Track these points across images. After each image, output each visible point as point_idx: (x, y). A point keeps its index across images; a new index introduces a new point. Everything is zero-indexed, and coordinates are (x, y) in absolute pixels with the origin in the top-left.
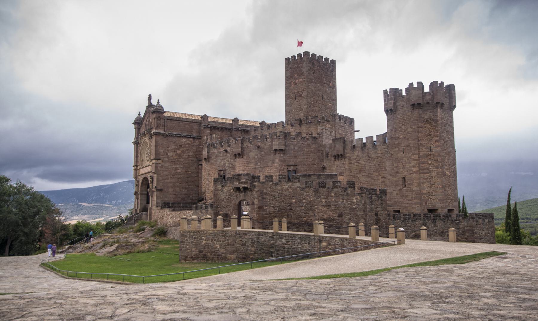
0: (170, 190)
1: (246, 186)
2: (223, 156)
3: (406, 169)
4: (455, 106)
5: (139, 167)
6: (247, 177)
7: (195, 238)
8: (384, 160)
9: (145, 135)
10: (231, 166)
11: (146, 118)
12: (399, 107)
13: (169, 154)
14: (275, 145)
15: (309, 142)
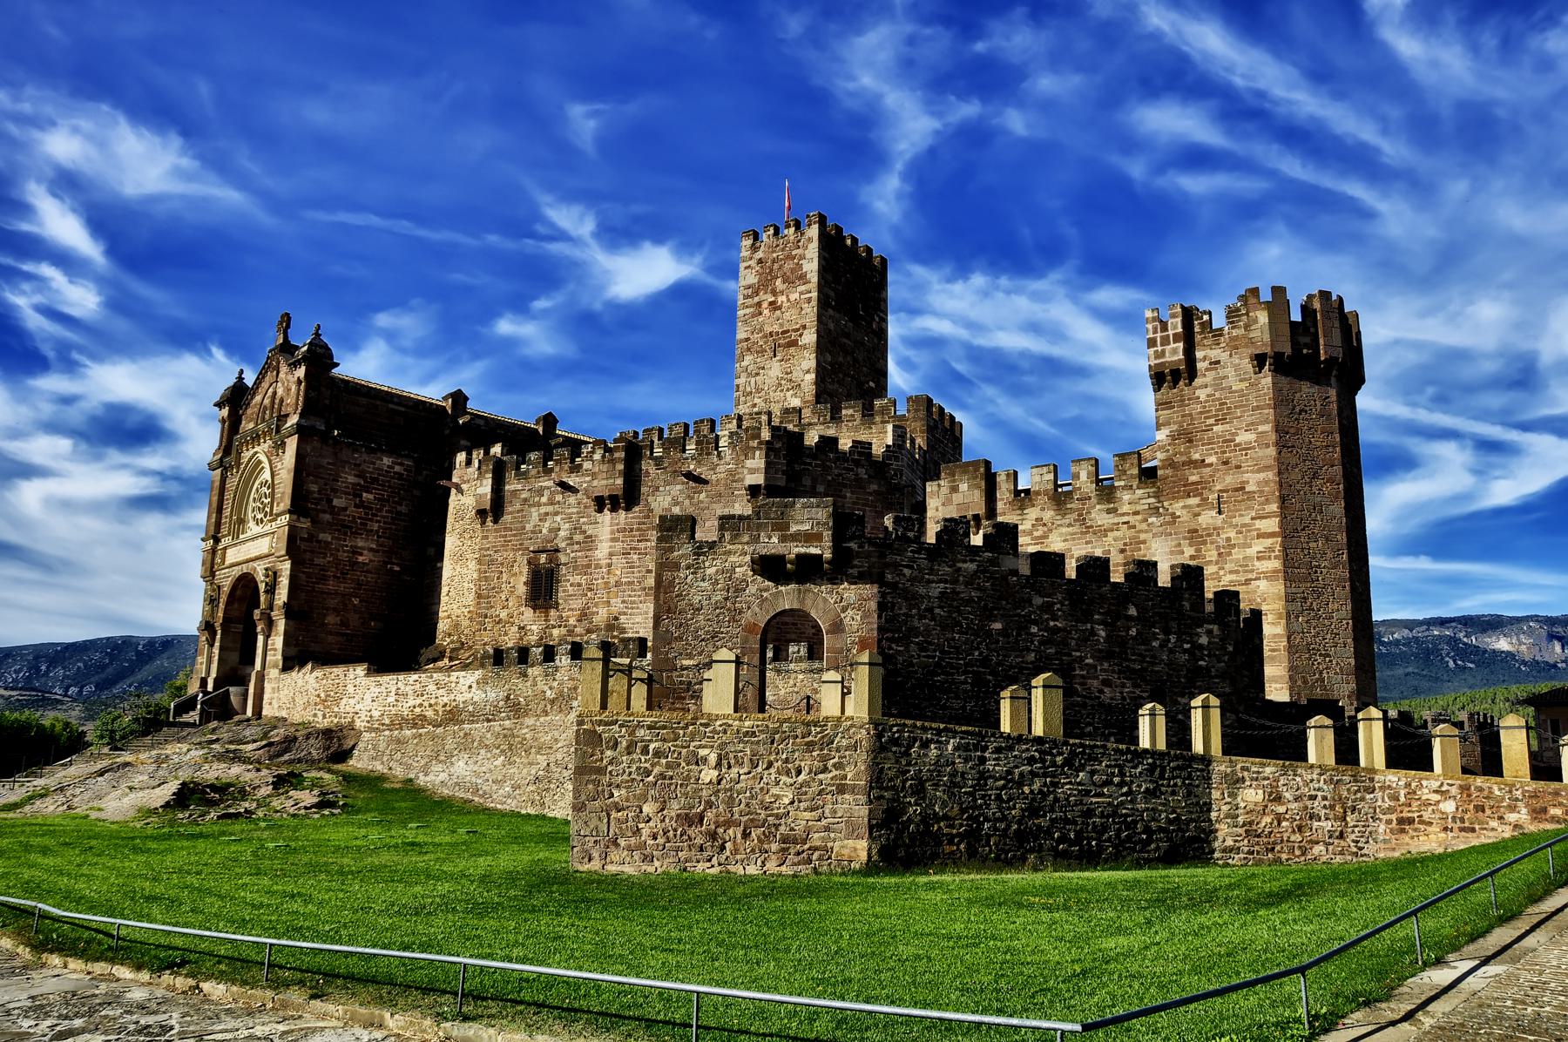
0: (331, 619)
1: (814, 551)
2: (551, 502)
3: (1228, 567)
4: (1363, 381)
5: (224, 542)
7: (657, 754)
8: (1143, 536)
9: (256, 438)
10: (578, 537)
11: (265, 385)
12: (1200, 366)
13: (336, 502)
14: (752, 471)
15: (862, 471)
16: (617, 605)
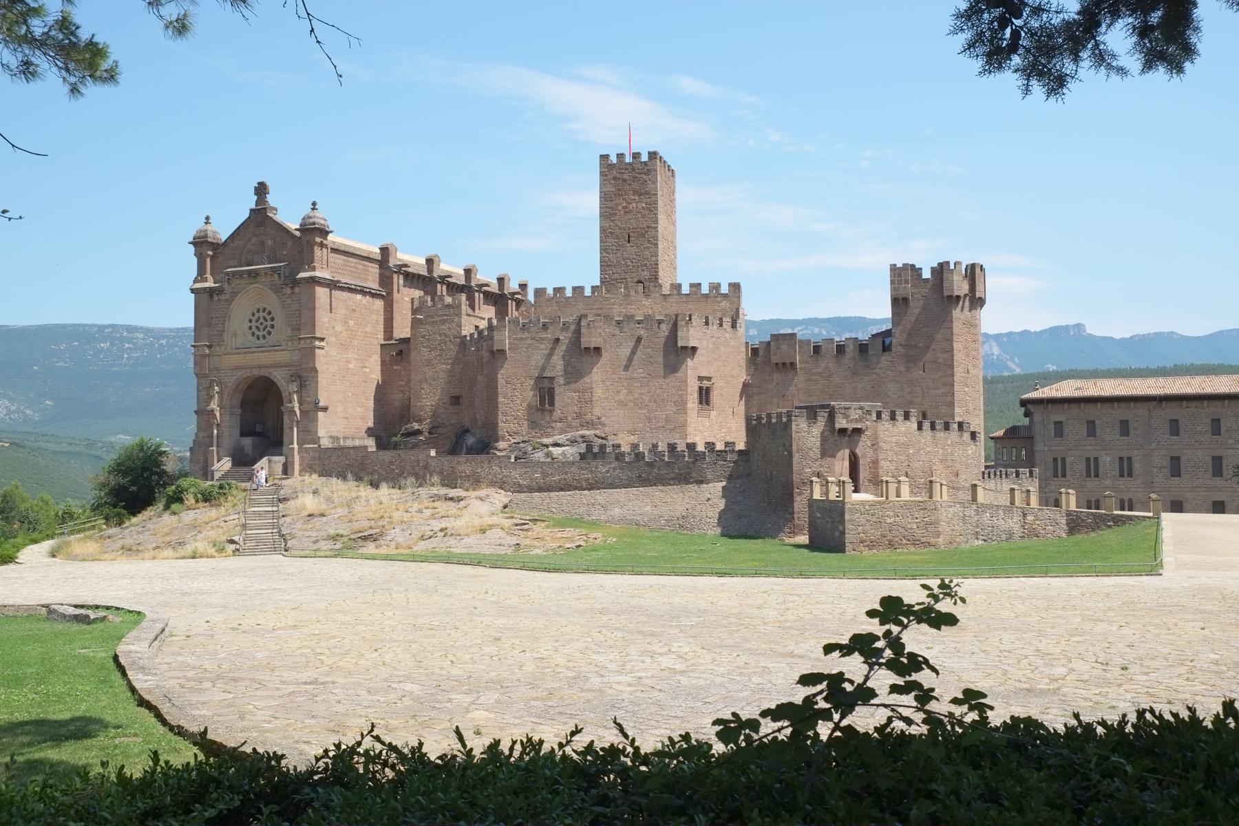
6: (860, 412)
16: (597, 411)
